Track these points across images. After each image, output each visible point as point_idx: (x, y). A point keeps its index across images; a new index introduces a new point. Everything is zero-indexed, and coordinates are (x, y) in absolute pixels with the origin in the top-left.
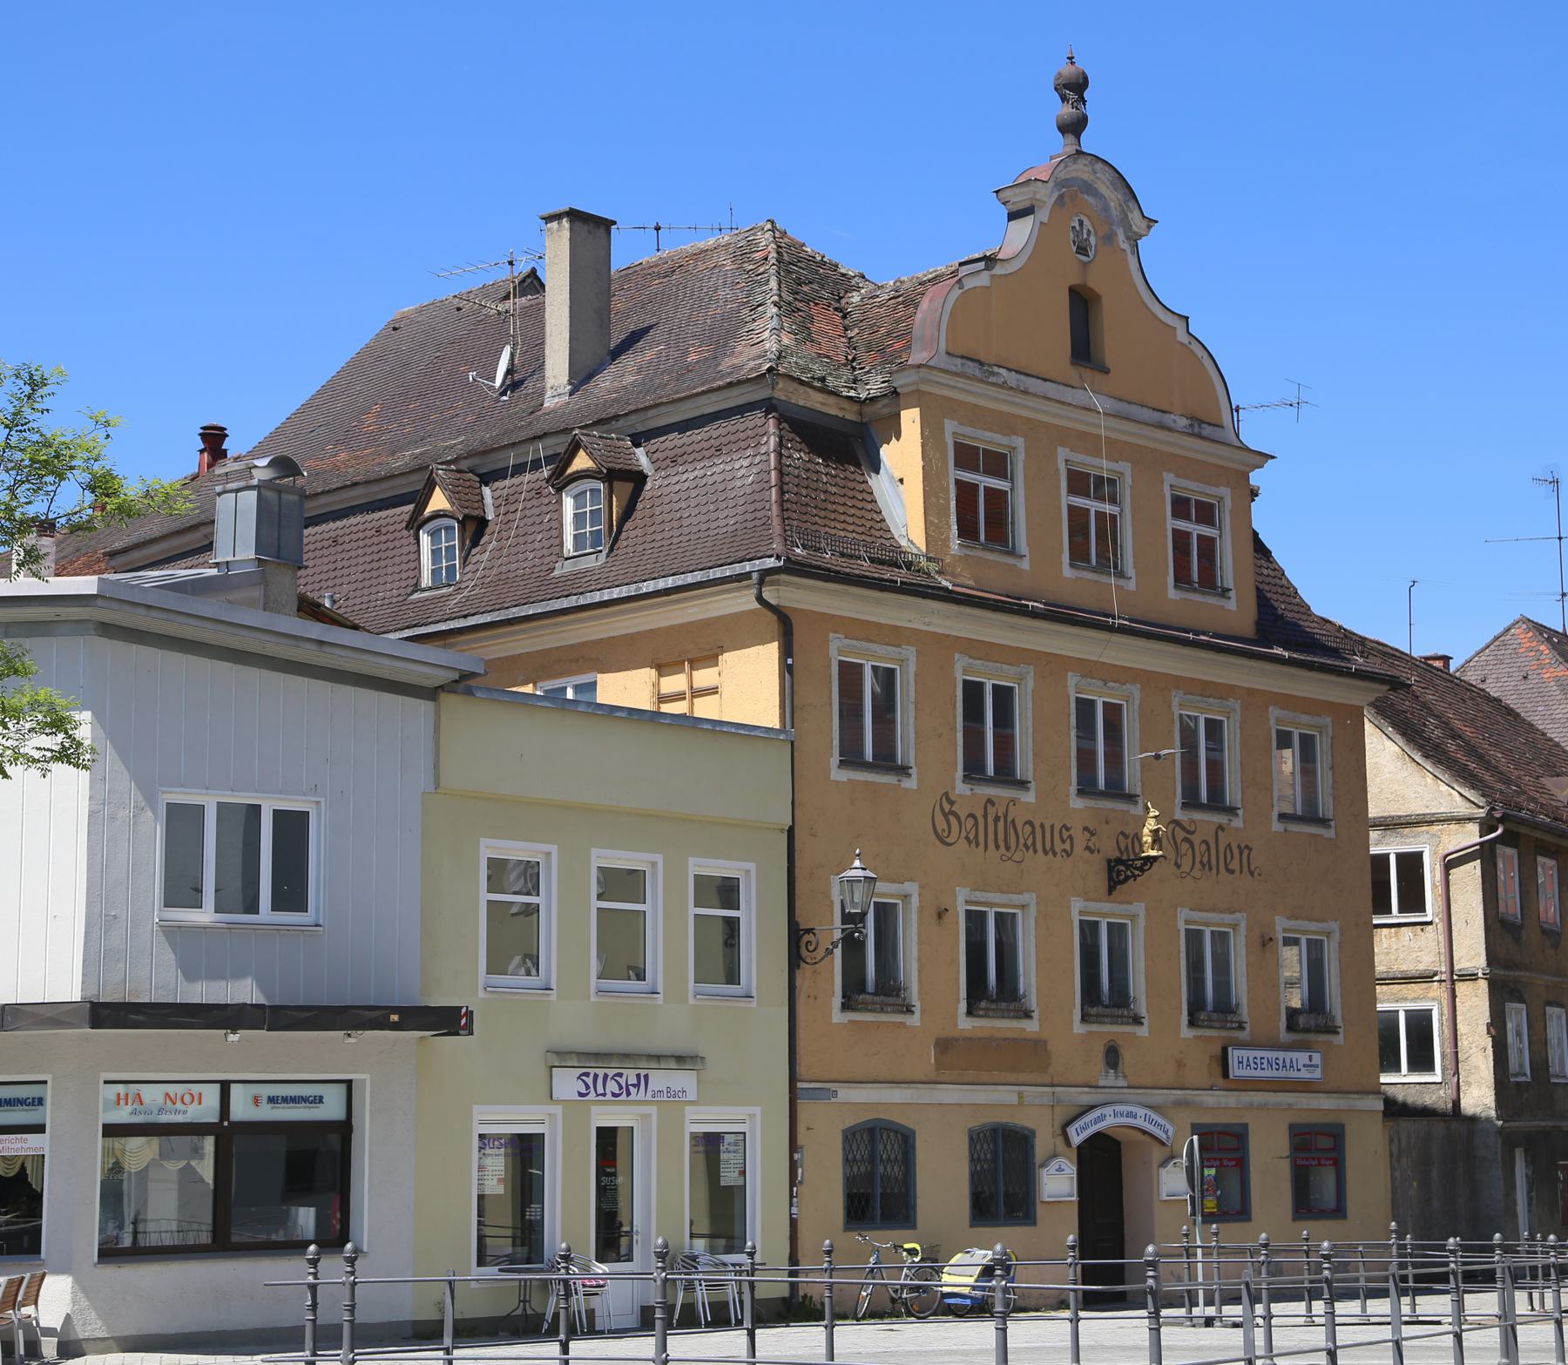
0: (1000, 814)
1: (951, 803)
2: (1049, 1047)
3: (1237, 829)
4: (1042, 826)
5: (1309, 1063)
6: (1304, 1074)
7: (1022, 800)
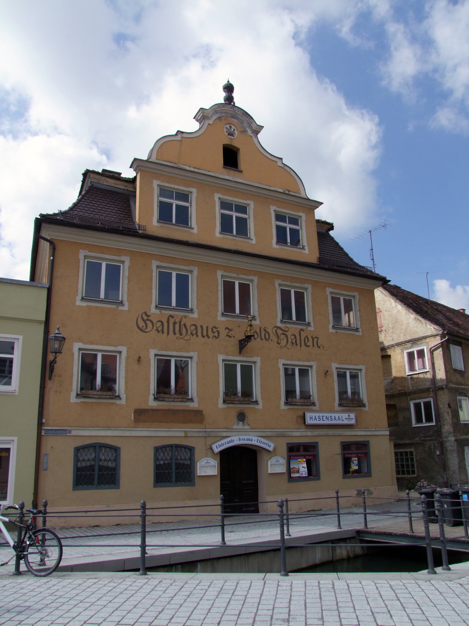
0: (177, 321)
1: (148, 316)
2: (204, 413)
3: (311, 331)
4: (202, 327)
5: (348, 417)
6: (346, 422)
7: (190, 316)
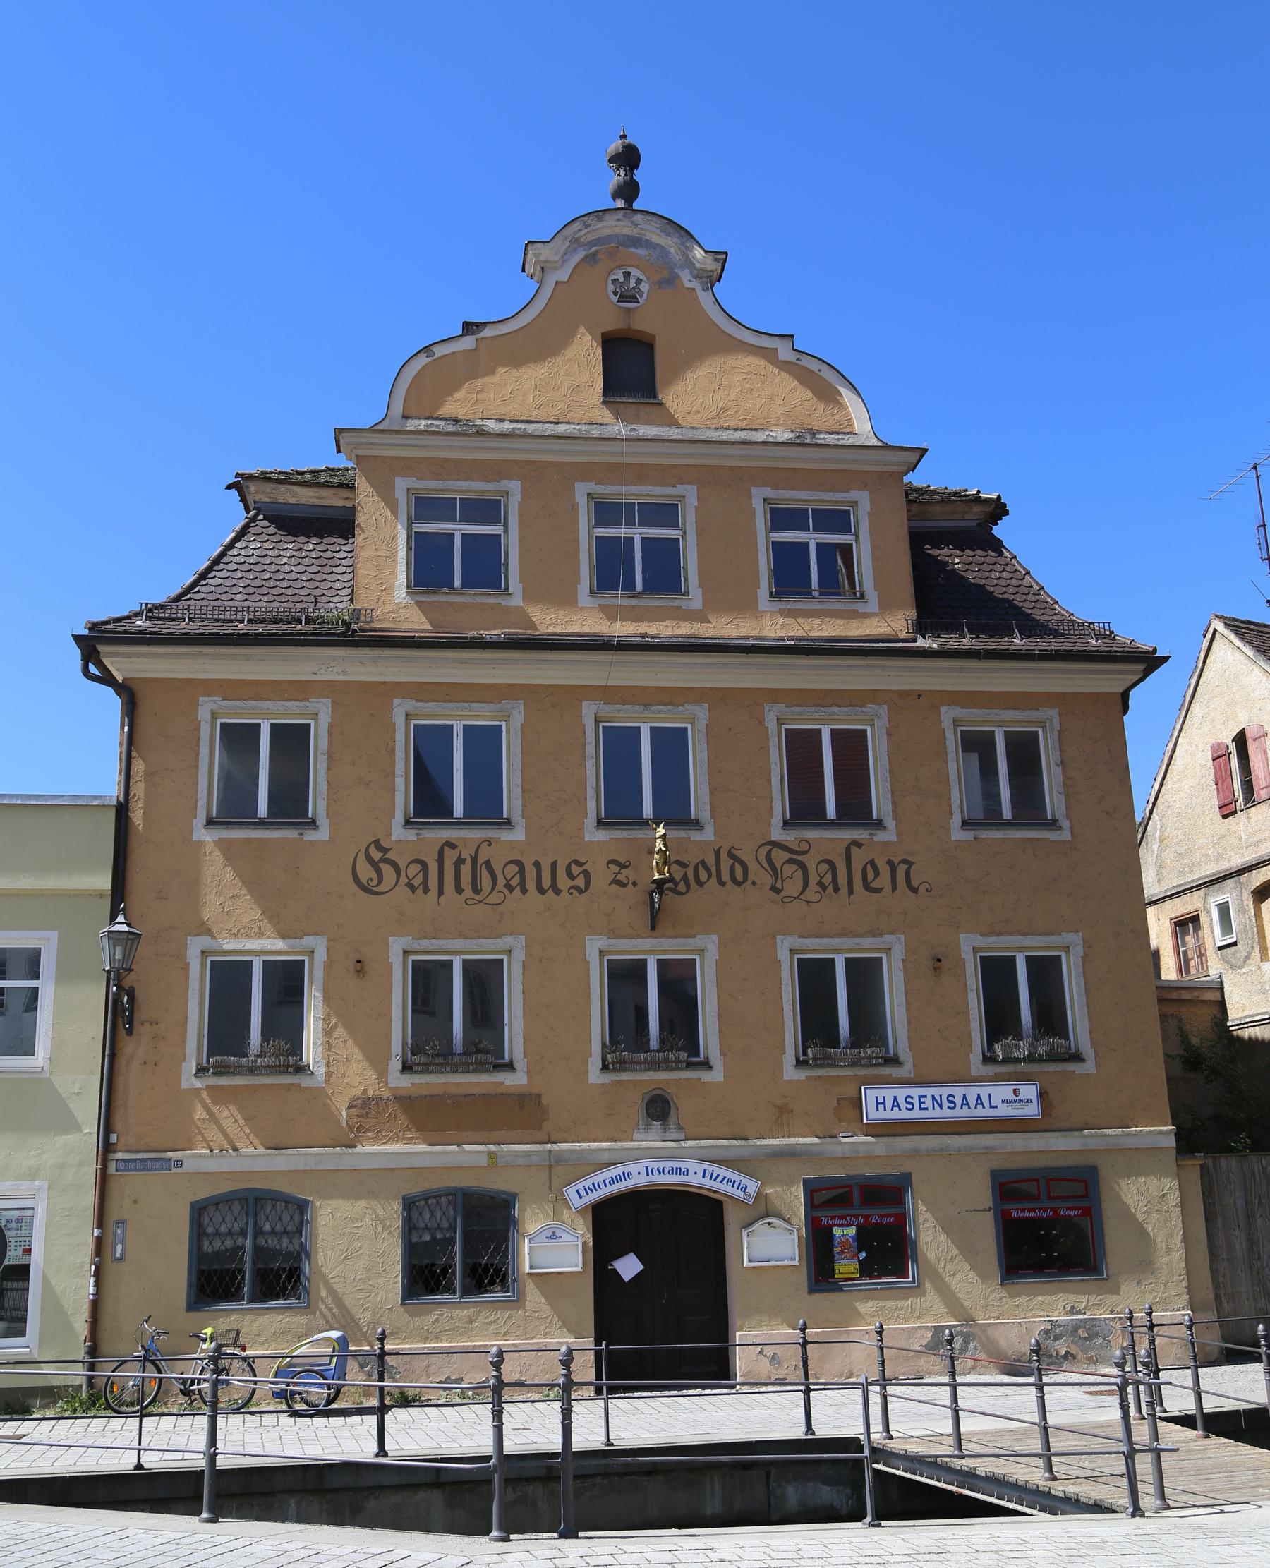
1: (385, 851)
2: (544, 1101)
3: (885, 844)
4: (537, 865)
6: (1004, 1111)
7: (502, 839)
